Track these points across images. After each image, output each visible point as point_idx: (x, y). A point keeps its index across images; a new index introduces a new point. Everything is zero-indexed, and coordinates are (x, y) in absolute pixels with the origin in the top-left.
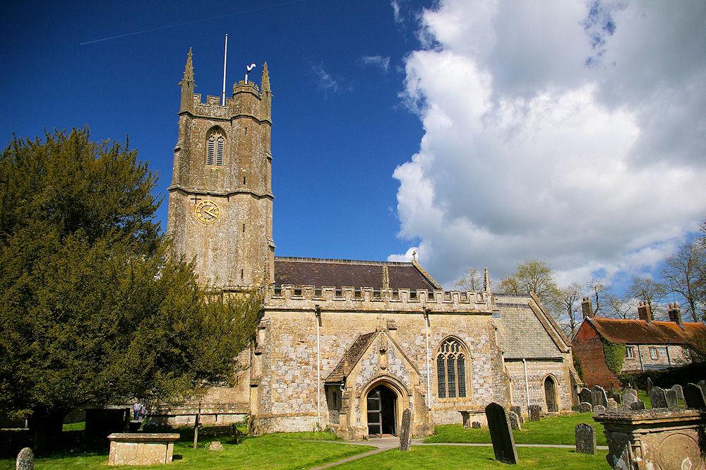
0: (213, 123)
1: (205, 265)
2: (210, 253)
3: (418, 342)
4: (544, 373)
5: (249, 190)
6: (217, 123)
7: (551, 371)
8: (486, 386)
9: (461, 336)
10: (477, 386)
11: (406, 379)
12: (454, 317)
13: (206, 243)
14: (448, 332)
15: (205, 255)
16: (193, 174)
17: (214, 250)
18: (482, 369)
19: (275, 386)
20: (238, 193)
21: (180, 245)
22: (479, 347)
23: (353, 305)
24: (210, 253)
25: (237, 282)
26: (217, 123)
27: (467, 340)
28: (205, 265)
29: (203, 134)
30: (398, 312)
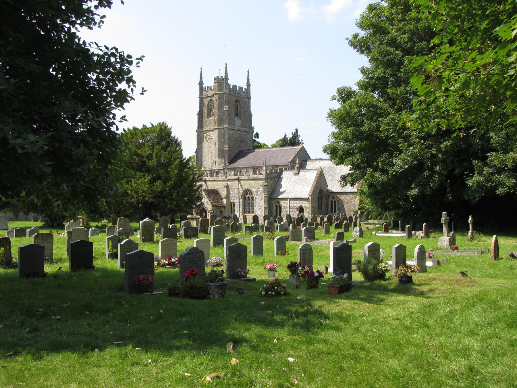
3: (236, 192)
4: (299, 205)
7: (301, 204)
8: (261, 210)
9: (252, 189)
10: (257, 210)
11: (208, 206)
12: (249, 182)
14: (245, 187)
17: (211, 153)
18: (260, 202)
22: (259, 193)
23: (216, 178)
24: (210, 155)
27: (254, 190)
30: (229, 180)
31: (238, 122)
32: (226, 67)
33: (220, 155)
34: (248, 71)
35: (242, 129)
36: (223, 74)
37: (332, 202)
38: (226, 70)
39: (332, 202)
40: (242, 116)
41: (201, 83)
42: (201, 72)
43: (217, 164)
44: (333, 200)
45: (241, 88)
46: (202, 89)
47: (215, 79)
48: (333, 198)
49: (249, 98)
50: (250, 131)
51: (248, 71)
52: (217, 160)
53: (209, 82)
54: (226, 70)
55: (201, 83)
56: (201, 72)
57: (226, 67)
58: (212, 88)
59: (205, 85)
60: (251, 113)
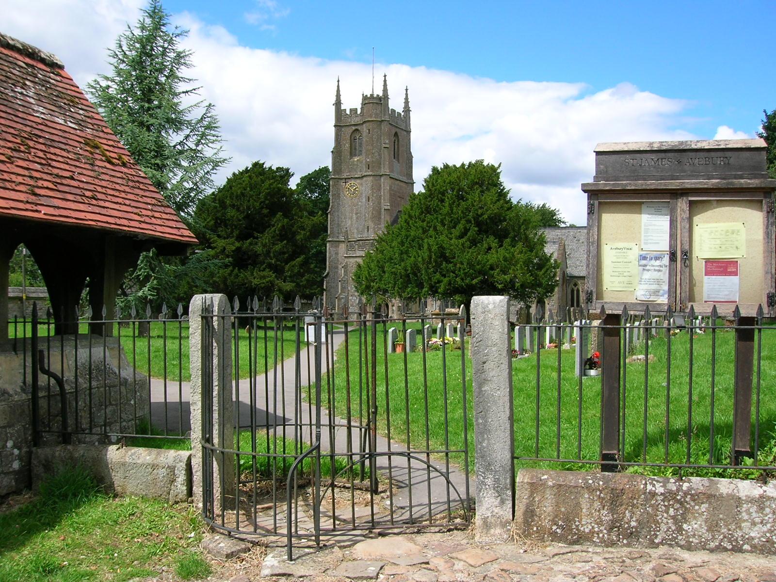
0: (354, 128)
1: (352, 224)
2: (354, 216)
5: (371, 173)
6: (356, 127)
13: (352, 210)
15: (351, 218)
16: (344, 167)
17: (356, 214)
19: (350, 298)
20: (365, 176)
21: (337, 213)
25: (365, 235)
26: (356, 127)
28: (352, 224)
29: (348, 137)
31: (397, 166)
32: (385, 81)
33: (377, 217)
34: (407, 90)
35: (401, 178)
36: (379, 92)
37: (573, 291)
38: (385, 85)
39: (573, 291)
40: (400, 156)
41: (338, 103)
42: (338, 86)
43: (371, 230)
44: (575, 289)
45: (399, 114)
46: (339, 112)
47: (365, 98)
48: (575, 285)
49: (409, 132)
50: (410, 181)
51: (407, 90)
52: (371, 225)
53: (352, 102)
54: (385, 85)
55: (338, 103)
56: (338, 86)
57: (385, 81)
58: (359, 112)
59: (346, 106)
60: (411, 153)
